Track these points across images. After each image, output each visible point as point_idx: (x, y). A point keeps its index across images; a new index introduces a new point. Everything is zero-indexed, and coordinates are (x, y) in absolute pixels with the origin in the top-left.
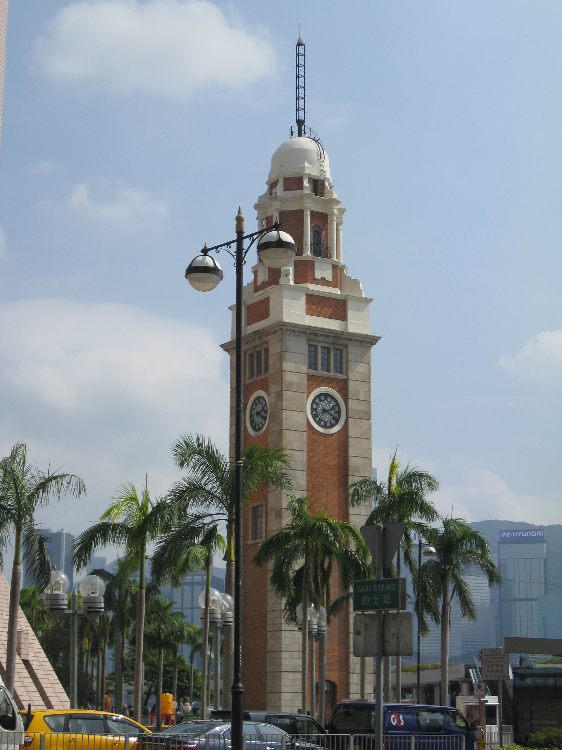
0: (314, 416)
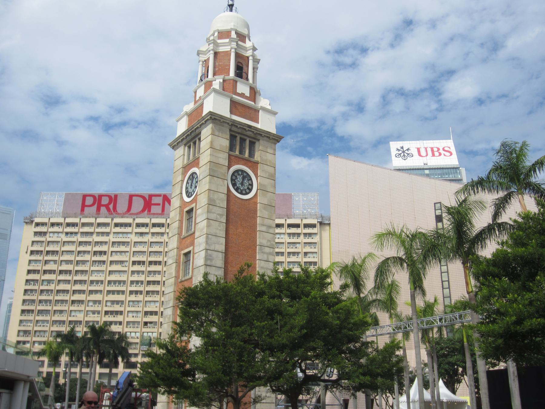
0: (234, 185)
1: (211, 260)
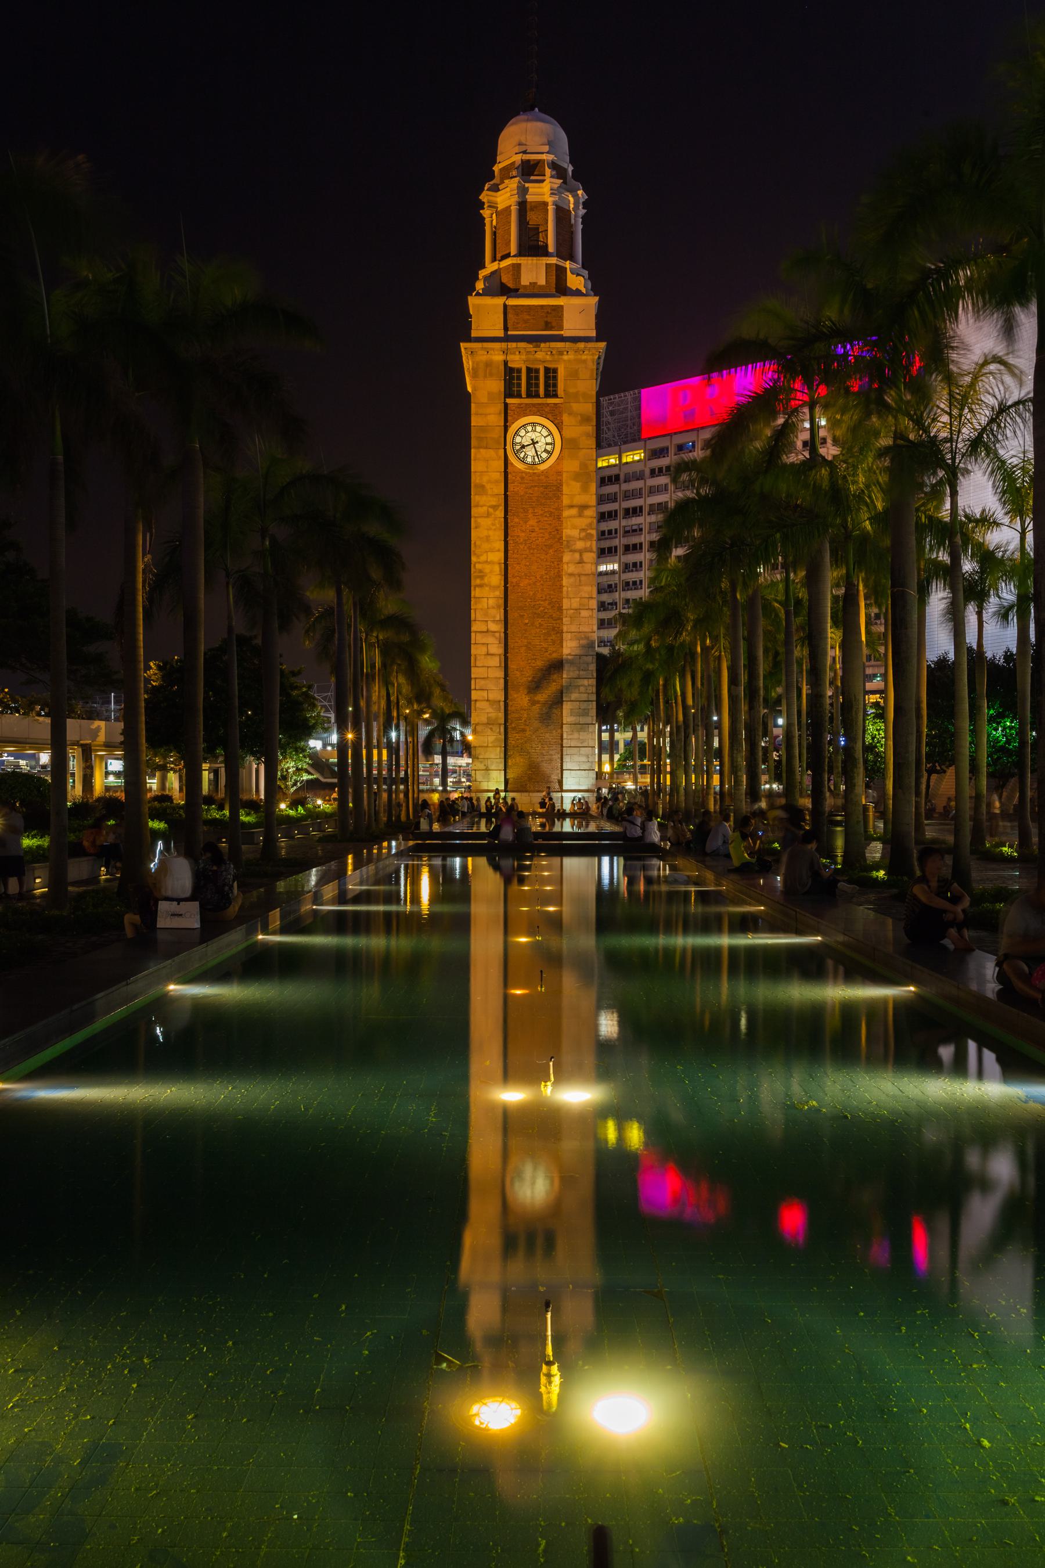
1: (482, 577)
